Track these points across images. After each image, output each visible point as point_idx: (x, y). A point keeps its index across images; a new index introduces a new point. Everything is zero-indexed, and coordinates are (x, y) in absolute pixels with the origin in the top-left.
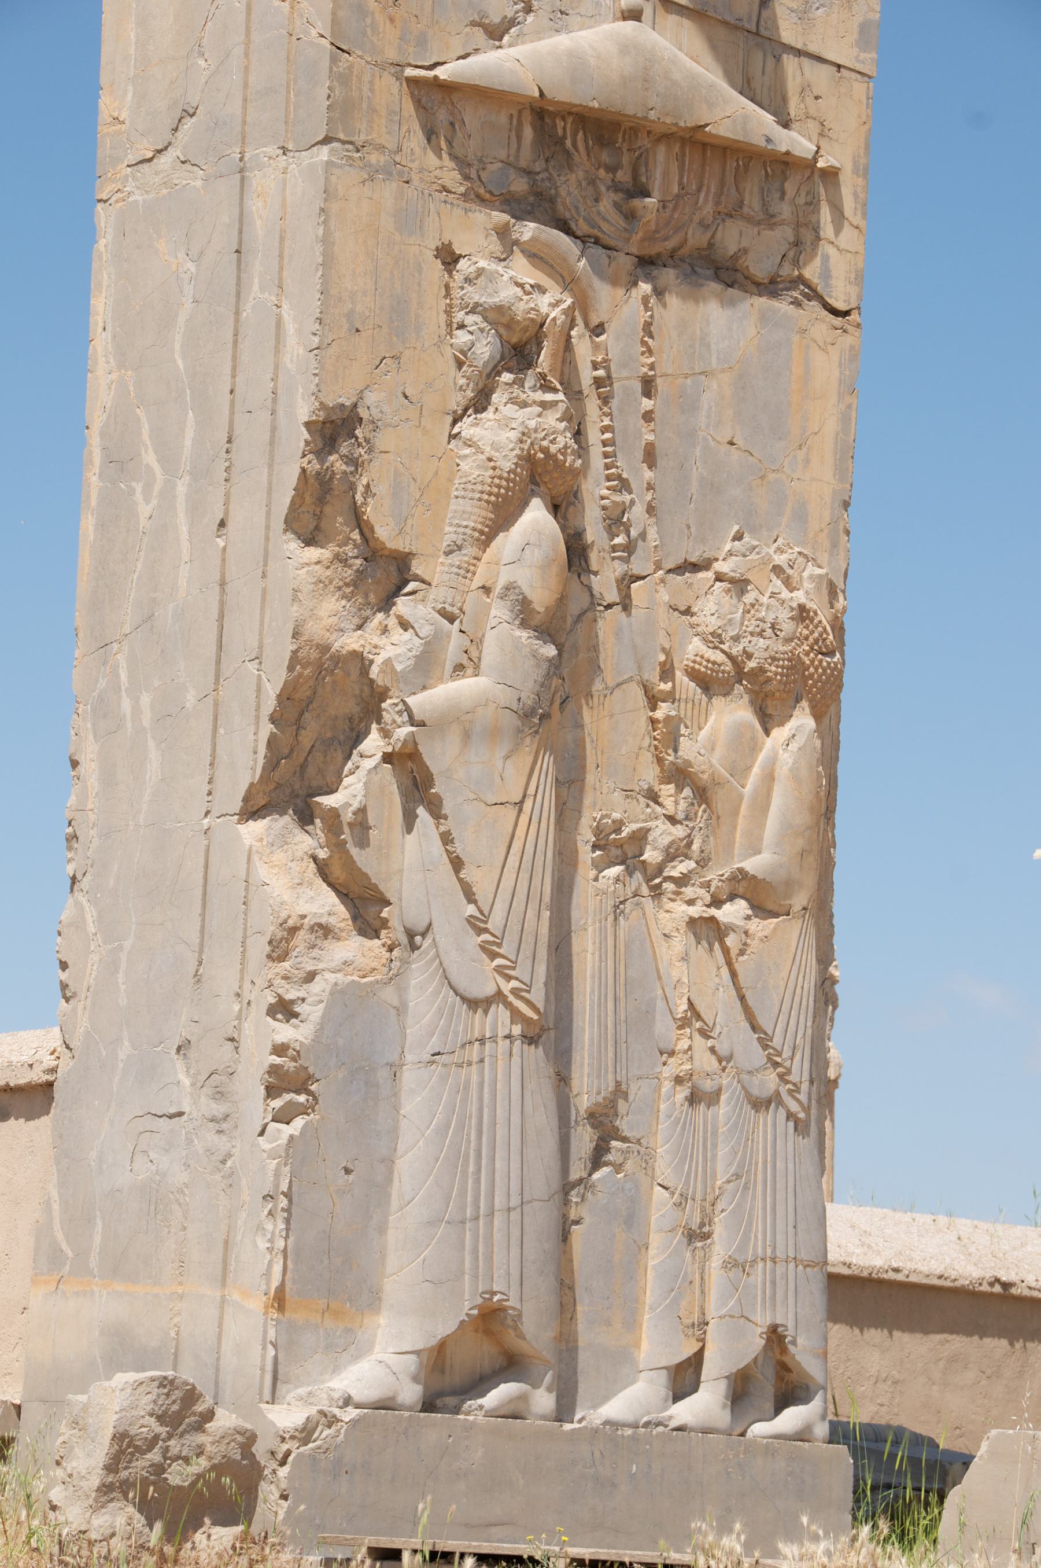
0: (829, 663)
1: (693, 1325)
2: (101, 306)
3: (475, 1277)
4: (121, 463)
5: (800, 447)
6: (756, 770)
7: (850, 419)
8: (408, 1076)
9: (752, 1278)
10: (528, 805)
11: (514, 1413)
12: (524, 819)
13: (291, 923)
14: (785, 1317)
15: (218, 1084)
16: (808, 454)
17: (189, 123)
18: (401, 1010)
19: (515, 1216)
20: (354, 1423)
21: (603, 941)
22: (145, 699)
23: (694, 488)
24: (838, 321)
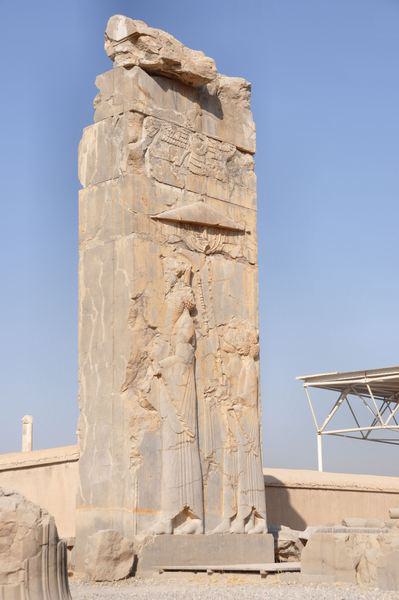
2: (81, 273)
4: (87, 310)
8: (164, 452)
15: (118, 458)
17: (100, 231)
18: (161, 437)
22: (96, 365)
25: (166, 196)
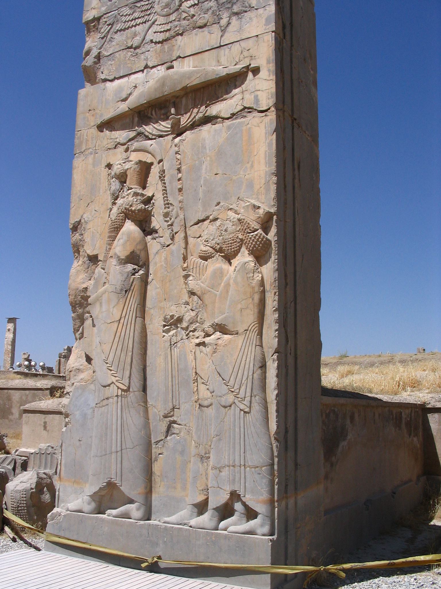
0: (252, 236)
1: (203, 490)
5: (248, 163)
6: (222, 284)
7: (272, 144)
9: (223, 474)
10: (122, 321)
12: (121, 325)
13: (70, 370)
16: (252, 164)
19: (119, 454)
21: (166, 357)
23: (201, 195)
24: (263, 114)
25: (120, 89)
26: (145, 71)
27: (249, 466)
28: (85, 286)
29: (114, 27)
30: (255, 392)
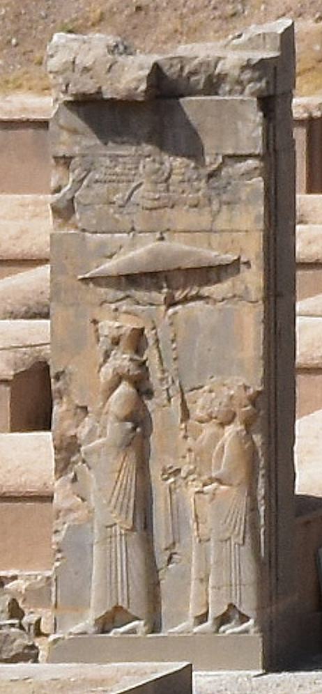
3: (111, 598)
11: (133, 631)
14: (236, 602)
20: (70, 639)
23: (195, 365)
25: (103, 245)
26: (131, 234)
27: (244, 585)
28: (72, 433)
29: (91, 174)
30: (247, 529)
